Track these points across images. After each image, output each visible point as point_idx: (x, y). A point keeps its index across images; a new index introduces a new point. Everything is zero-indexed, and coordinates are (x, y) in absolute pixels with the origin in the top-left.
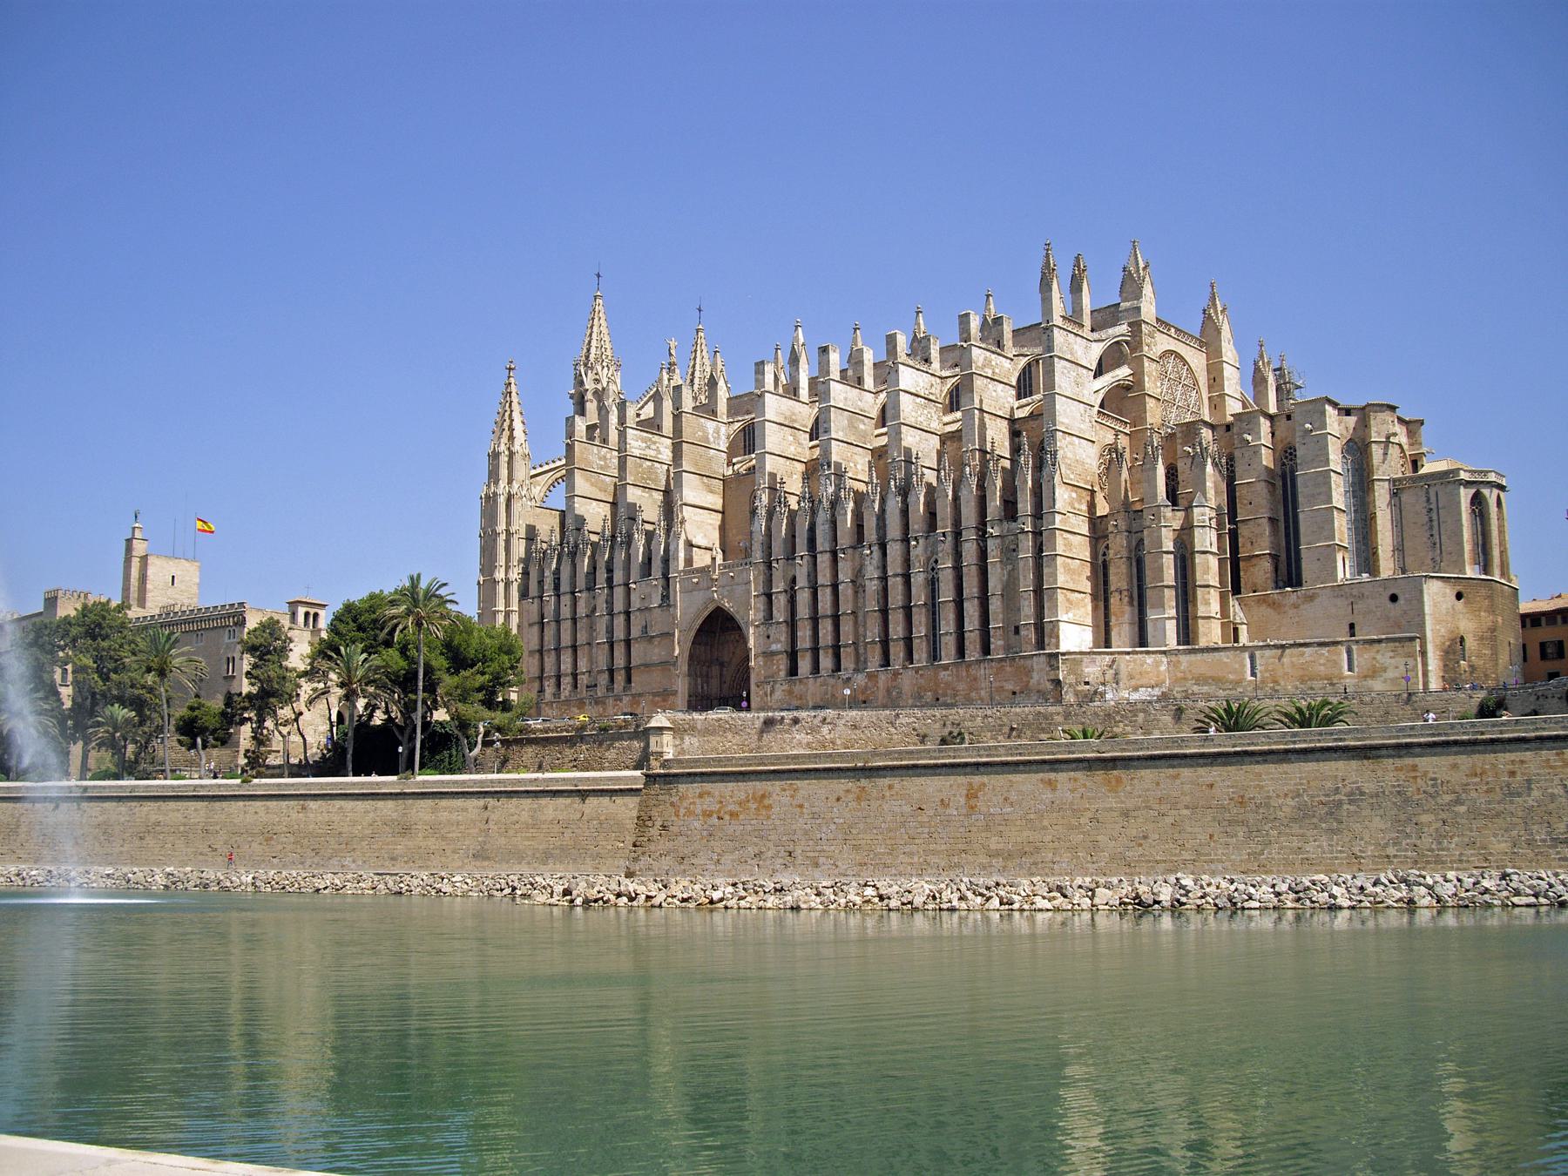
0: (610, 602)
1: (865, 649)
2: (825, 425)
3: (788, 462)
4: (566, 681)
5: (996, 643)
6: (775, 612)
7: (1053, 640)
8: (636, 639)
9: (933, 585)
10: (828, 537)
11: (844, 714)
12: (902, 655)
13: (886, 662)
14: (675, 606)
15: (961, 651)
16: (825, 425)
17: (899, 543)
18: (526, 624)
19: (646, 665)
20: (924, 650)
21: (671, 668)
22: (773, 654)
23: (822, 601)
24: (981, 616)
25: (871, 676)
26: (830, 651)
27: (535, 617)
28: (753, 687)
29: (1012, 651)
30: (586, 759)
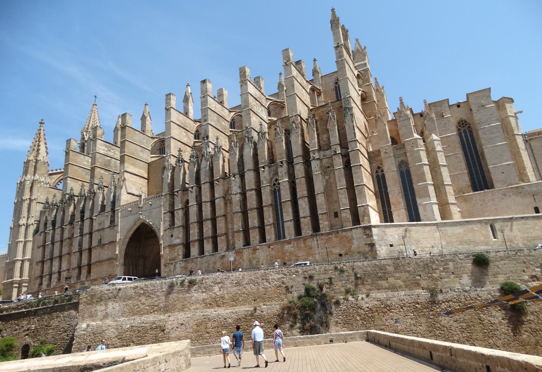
0: (82, 229)
1: (233, 237)
2: (205, 118)
3: (183, 145)
4: (55, 277)
5: (324, 224)
6: (176, 221)
7: (366, 218)
8: (95, 247)
9: (276, 193)
10: (208, 174)
11: (230, 274)
12: (258, 237)
13: (247, 243)
14: (117, 225)
15: (298, 231)
16: (205, 118)
17: (252, 171)
18: (36, 247)
19: (100, 262)
20: (273, 233)
21: (114, 261)
22: (175, 246)
23: (205, 211)
24: (310, 208)
25: (239, 253)
26: (211, 240)
27: (41, 243)
28: (162, 267)
29: (335, 229)
30: (36, 328)
